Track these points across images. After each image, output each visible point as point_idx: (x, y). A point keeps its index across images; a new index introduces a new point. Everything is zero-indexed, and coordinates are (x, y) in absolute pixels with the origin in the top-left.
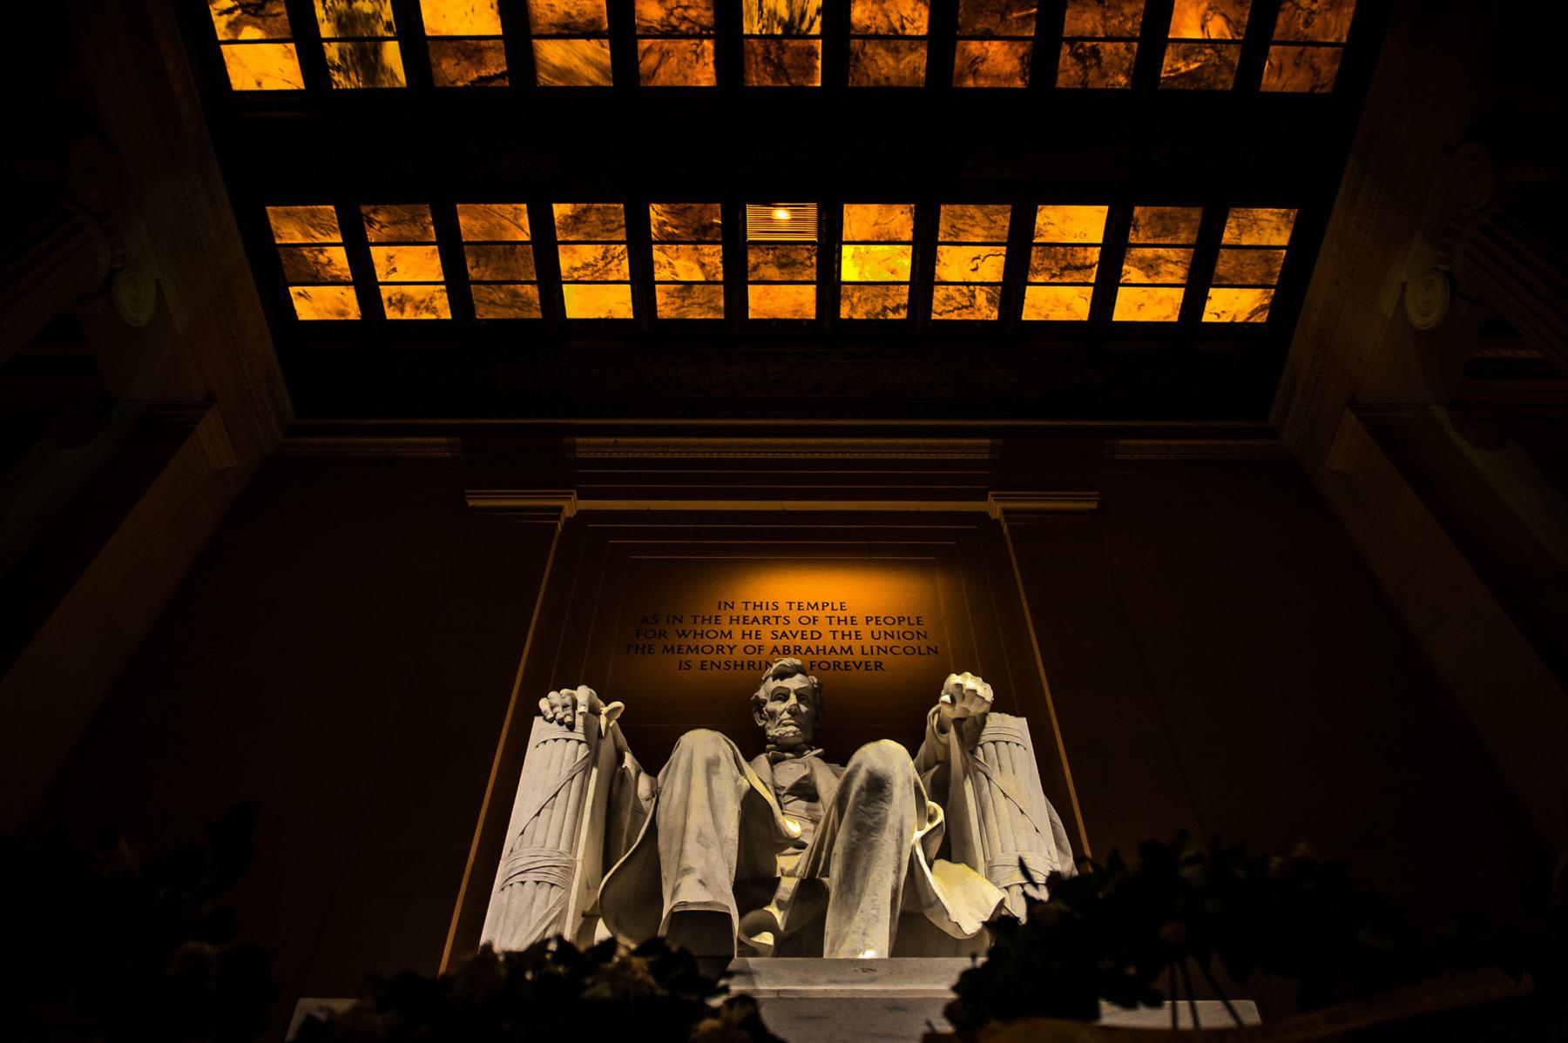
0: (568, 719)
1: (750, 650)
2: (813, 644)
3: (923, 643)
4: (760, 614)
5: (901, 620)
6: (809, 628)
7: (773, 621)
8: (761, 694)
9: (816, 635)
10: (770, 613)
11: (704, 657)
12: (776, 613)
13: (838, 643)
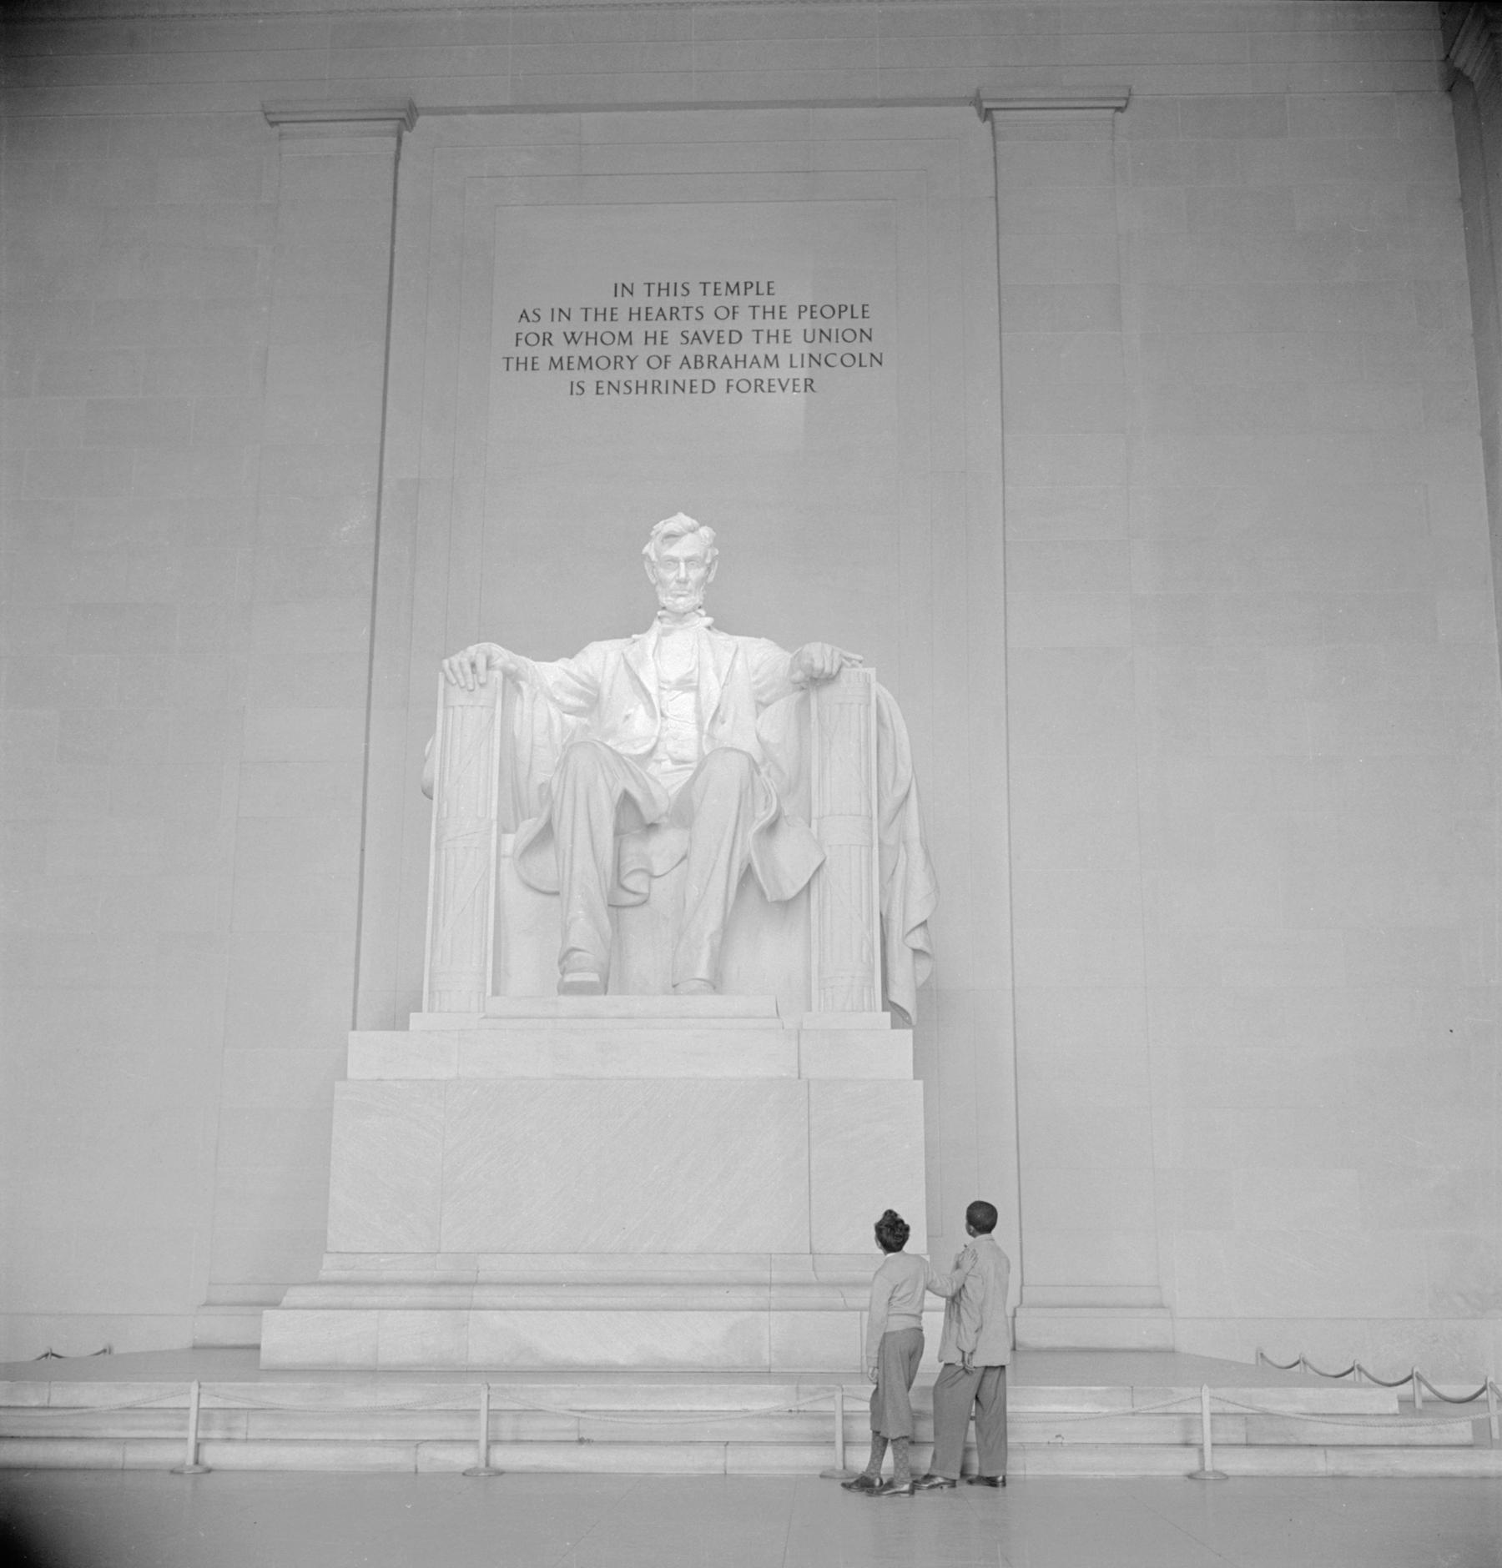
1: (654, 362)
2: (730, 351)
3: (863, 348)
4: (667, 302)
5: (840, 311)
6: (729, 324)
7: (682, 314)
8: (649, 549)
9: (735, 337)
10: (679, 301)
11: (596, 374)
12: (688, 301)
13: (763, 349)
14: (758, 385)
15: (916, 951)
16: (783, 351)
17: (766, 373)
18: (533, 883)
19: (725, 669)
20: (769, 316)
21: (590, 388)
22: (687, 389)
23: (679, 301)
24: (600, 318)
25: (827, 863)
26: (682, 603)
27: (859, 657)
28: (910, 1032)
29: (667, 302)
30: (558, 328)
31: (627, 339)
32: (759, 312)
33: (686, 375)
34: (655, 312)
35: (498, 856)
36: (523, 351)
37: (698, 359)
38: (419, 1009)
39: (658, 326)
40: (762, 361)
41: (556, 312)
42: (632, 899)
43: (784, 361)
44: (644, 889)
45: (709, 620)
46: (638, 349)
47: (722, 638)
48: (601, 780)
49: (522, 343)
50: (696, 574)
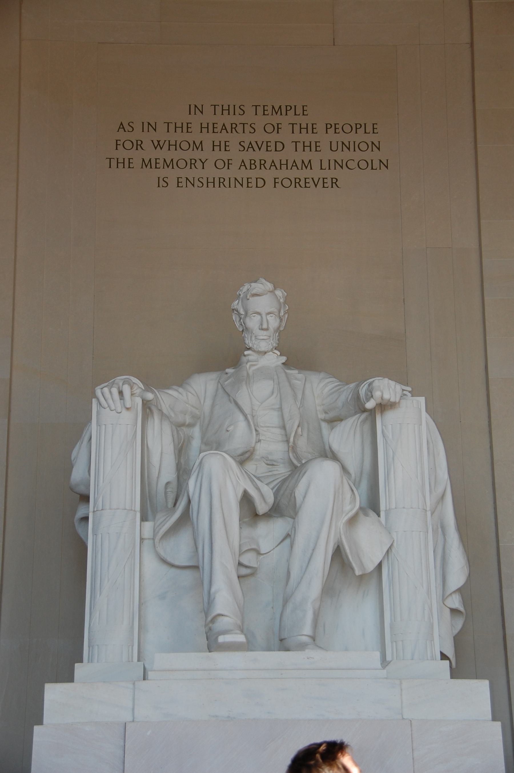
0: (119, 411)
1: (220, 164)
2: (277, 157)
3: (375, 156)
4: (228, 120)
5: (357, 127)
6: (273, 137)
7: (240, 128)
9: (279, 146)
10: (238, 119)
14: (297, 182)
15: (454, 611)
16: (315, 157)
17: (303, 174)
18: (170, 559)
19: (300, 396)
20: (304, 131)
21: (173, 182)
22: (245, 184)
23: (238, 119)
24: (179, 130)
25: (395, 544)
26: (263, 346)
27: (410, 389)
28: (486, 682)
29: (228, 120)
30: (147, 138)
31: (199, 146)
32: (297, 128)
33: (243, 174)
34: (219, 127)
35: (142, 539)
36: (122, 154)
37: (252, 163)
38: (82, 661)
39: (223, 136)
40: (299, 165)
41: (146, 125)
42: (244, 571)
43: (316, 165)
44: (253, 564)
45: (284, 359)
46: (207, 153)
47: (295, 372)
48: (229, 483)
49: (120, 147)
50: (273, 322)
